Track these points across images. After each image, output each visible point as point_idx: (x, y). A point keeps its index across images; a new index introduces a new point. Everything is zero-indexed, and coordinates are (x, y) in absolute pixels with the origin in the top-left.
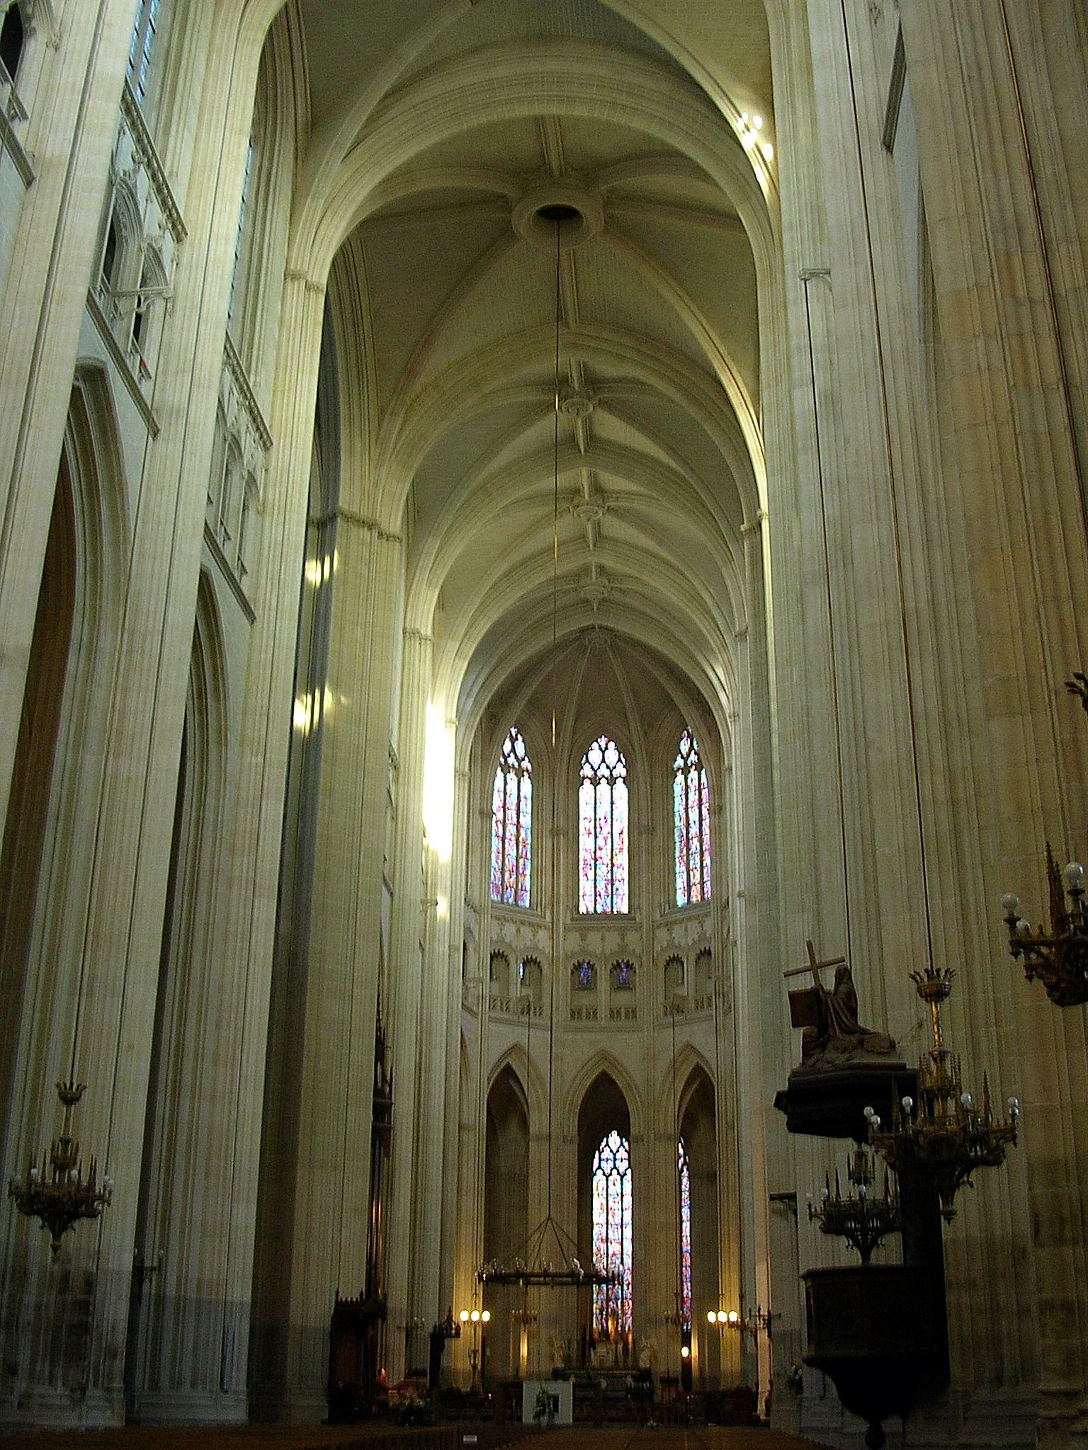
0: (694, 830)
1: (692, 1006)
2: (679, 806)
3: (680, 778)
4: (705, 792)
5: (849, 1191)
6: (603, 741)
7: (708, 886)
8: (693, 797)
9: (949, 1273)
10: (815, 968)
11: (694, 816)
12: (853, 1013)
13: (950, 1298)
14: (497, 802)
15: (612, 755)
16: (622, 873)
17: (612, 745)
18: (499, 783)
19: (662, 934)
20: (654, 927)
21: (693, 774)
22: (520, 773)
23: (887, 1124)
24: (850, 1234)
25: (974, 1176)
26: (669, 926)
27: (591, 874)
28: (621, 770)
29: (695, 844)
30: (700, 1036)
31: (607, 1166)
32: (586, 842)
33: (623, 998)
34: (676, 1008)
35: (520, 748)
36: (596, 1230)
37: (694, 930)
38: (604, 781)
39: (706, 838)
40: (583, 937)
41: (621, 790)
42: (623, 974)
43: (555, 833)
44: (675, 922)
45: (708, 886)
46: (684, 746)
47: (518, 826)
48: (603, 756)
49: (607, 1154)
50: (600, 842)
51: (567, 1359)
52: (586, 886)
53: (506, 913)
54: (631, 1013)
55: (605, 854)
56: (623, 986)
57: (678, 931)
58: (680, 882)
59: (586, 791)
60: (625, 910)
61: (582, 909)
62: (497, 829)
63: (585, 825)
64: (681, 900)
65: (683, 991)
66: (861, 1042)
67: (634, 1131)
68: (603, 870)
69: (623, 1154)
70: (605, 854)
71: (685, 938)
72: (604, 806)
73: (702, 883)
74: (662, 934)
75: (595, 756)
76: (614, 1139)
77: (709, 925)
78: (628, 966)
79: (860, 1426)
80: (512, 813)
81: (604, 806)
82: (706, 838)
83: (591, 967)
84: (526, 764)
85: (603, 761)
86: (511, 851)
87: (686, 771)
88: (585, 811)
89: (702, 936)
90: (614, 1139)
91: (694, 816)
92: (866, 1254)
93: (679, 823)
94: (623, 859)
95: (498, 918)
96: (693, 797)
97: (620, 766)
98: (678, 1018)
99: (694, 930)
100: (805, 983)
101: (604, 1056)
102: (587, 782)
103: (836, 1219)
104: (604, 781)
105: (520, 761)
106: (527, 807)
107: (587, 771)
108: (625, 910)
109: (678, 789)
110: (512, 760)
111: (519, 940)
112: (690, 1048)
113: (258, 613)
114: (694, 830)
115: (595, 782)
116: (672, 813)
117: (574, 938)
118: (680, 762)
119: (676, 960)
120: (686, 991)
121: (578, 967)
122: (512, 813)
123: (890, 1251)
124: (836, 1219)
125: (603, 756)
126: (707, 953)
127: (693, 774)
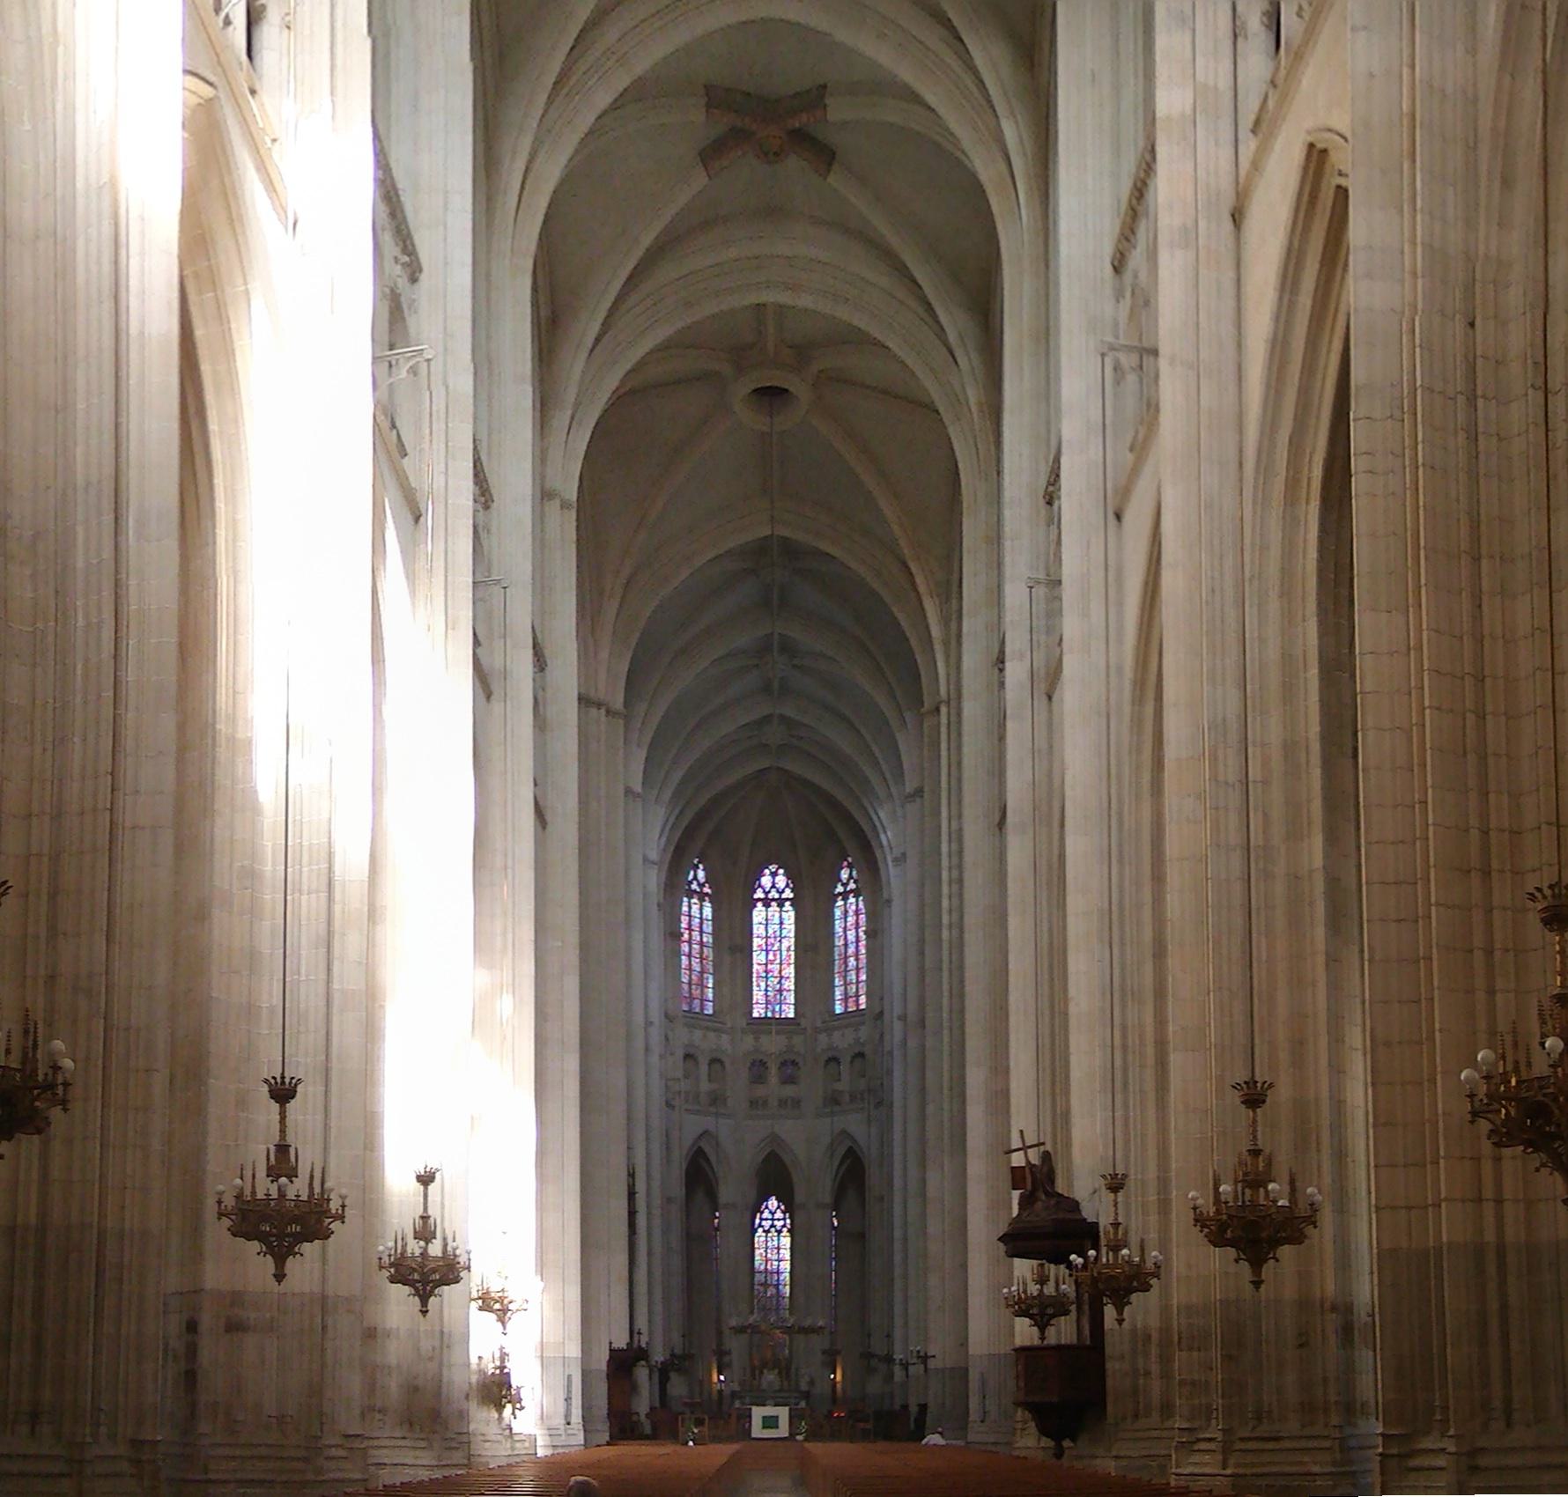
0: (851, 950)
1: (847, 1098)
2: (838, 928)
3: (840, 903)
4: (863, 917)
5: (1034, 1289)
6: (773, 868)
7: (863, 999)
8: (851, 920)
9: (1108, 1350)
10: (1025, 1148)
11: (851, 936)
12: (1052, 1181)
13: (1109, 1365)
14: (684, 925)
15: (781, 881)
16: (790, 984)
17: (781, 871)
18: (685, 909)
19: (823, 1038)
20: (817, 1031)
21: (852, 900)
22: (702, 897)
23: (1085, 1266)
24: (1031, 1317)
25: (1134, 1297)
26: (829, 1031)
27: (763, 985)
28: (788, 894)
29: (852, 962)
30: (855, 1124)
31: (767, 1224)
32: (758, 958)
33: (789, 1091)
34: (833, 1100)
35: (701, 875)
36: (759, 1278)
37: (850, 1036)
38: (774, 904)
39: (863, 957)
40: (757, 1039)
41: (790, 915)
42: (790, 1068)
43: (733, 949)
44: (835, 1028)
45: (863, 999)
46: (844, 875)
47: (701, 943)
48: (773, 880)
49: (766, 1214)
50: (771, 957)
51: (742, 1383)
52: (758, 995)
53: (694, 1019)
54: (797, 1103)
55: (775, 967)
56: (789, 1080)
57: (837, 1034)
58: (838, 994)
59: (759, 913)
60: (791, 1015)
61: (755, 1015)
62: (685, 948)
63: (756, 942)
64: (839, 1009)
65: (840, 1086)
66: (1058, 1203)
67: (799, 1197)
68: (773, 981)
69: (779, 1215)
70: (775, 967)
71: (843, 1040)
72: (774, 927)
73: (857, 996)
74: (823, 1038)
75: (766, 881)
76: (773, 1203)
77: (864, 1033)
78: (794, 1063)
79: (1047, 1442)
80: (696, 934)
81: (774, 927)
82: (863, 957)
83: (763, 1064)
84: (707, 890)
85: (773, 886)
86: (696, 967)
87: (845, 899)
88: (758, 930)
89: (857, 1040)
90: (773, 1203)
91: (851, 936)
92: (1042, 1330)
93: (839, 942)
94: (790, 971)
95: (686, 1025)
96: (851, 920)
97: (788, 891)
98: (837, 1108)
99: (850, 1036)
100: (1018, 1160)
101: (774, 1138)
102: (759, 904)
103: (1022, 1307)
104: (774, 904)
105: (701, 885)
106: (708, 927)
107: (759, 894)
108: (791, 1015)
109: (838, 913)
110: (694, 886)
111: (706, 1042)
112: (844, 1132)
113: (548, 818)
114: (851, 950)
115: (767, 903)
116: (832, 934)
117: (749, 1041)
118: (840, 889)
119: (834, 1060)
120: (843, 1085)
121: (753, 1064)
122: (696, 934)
123: (1064, 1331)
124: (1022, 1307)
125: (773, 880)
126: (861, 1055)
127: (852, 900)
